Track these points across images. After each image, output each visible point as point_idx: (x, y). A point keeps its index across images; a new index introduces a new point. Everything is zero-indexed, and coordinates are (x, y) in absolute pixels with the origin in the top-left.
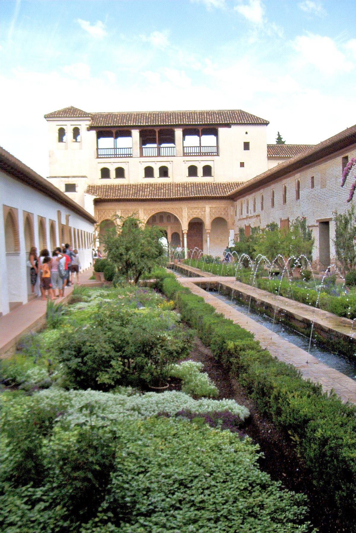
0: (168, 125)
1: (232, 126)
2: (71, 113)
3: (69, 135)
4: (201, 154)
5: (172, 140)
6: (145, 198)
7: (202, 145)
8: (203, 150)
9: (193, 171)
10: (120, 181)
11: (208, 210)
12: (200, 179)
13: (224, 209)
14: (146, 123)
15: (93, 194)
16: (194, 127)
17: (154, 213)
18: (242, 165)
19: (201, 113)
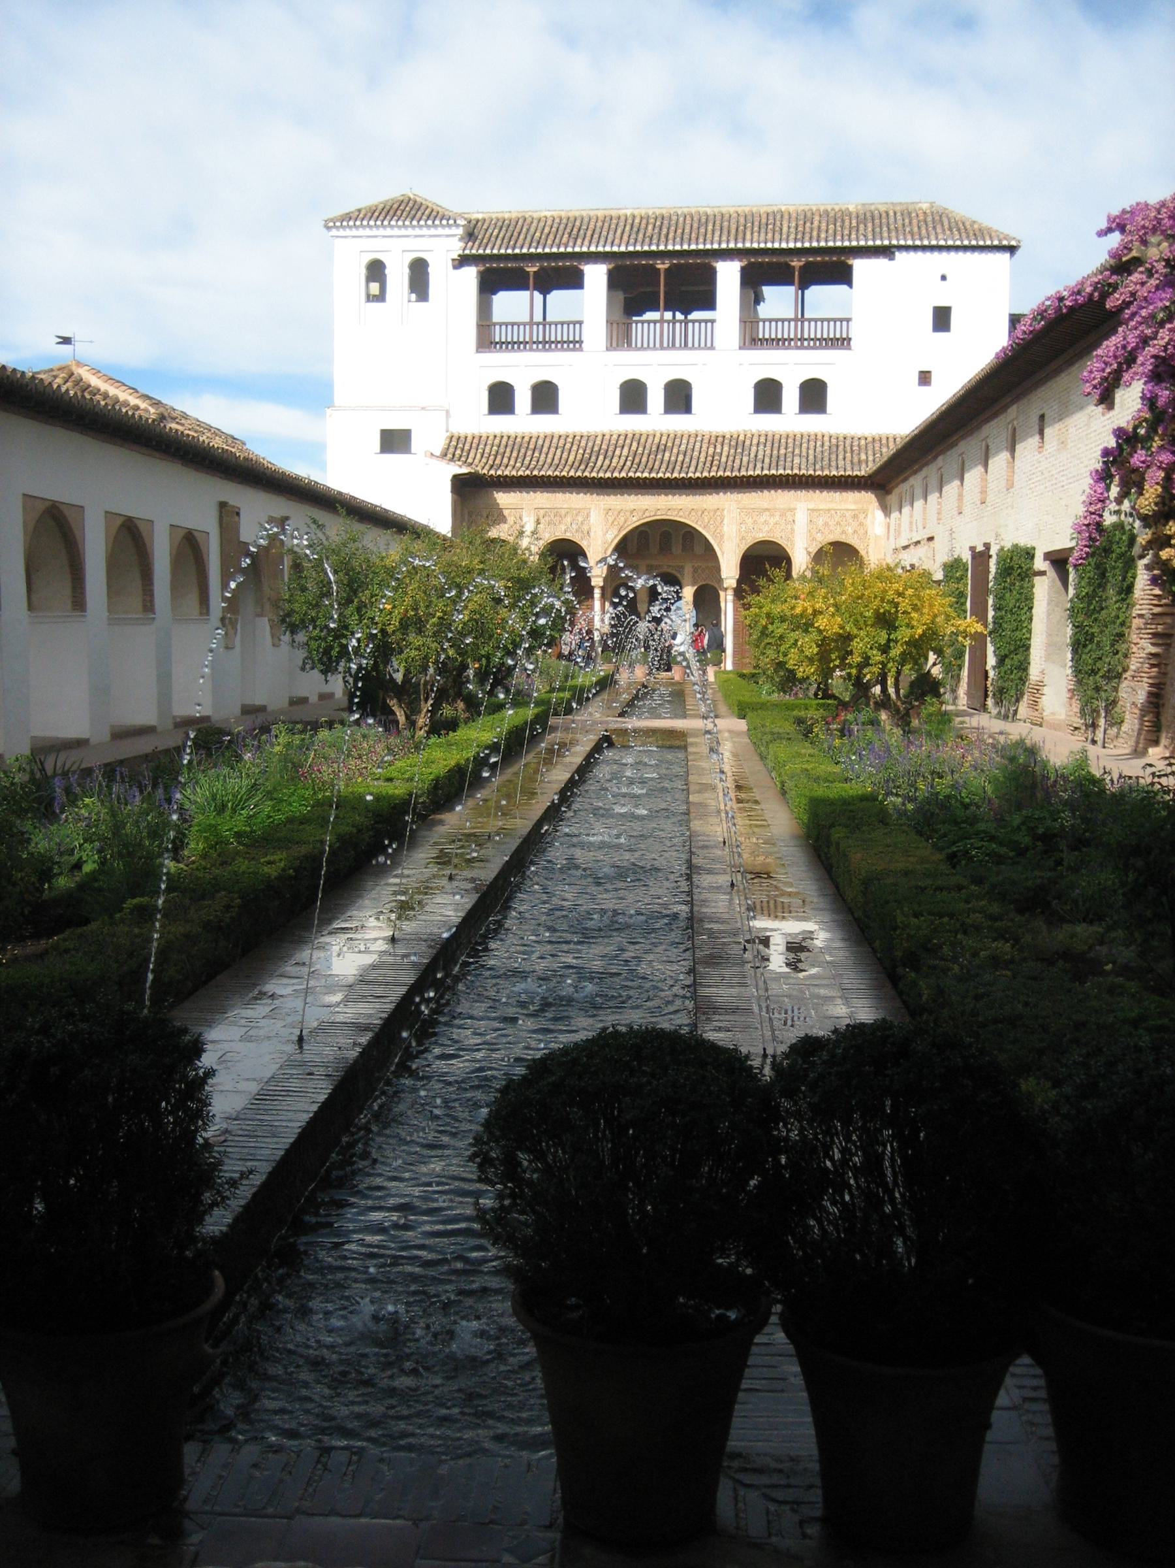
0: (697, 253)
1: (898, 255)
2: (406, 211)
3: (398, 277)
4: (801, 342)
5: (708, 301)
6: (608, 475)
7: (806, 316)
8: (810, 330)
9: (767, 396)
10: (544, 424)
11: (801, 517)
12: (790, 420)
13: (855, 517)
14: (627, 244)
15: (452, 460)
16: (782, 259)
17: (634, 522)
18: (925, 378)
19: (806, 217)
